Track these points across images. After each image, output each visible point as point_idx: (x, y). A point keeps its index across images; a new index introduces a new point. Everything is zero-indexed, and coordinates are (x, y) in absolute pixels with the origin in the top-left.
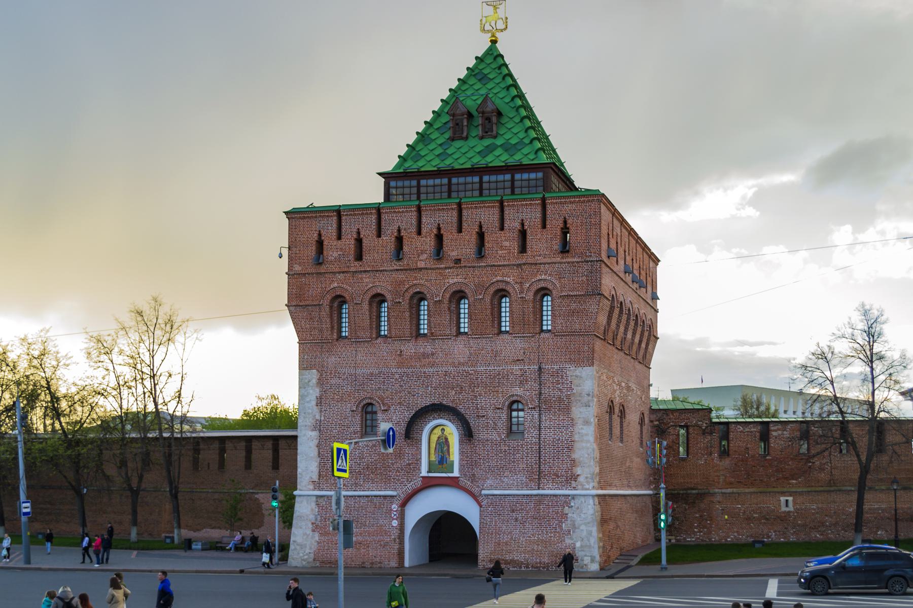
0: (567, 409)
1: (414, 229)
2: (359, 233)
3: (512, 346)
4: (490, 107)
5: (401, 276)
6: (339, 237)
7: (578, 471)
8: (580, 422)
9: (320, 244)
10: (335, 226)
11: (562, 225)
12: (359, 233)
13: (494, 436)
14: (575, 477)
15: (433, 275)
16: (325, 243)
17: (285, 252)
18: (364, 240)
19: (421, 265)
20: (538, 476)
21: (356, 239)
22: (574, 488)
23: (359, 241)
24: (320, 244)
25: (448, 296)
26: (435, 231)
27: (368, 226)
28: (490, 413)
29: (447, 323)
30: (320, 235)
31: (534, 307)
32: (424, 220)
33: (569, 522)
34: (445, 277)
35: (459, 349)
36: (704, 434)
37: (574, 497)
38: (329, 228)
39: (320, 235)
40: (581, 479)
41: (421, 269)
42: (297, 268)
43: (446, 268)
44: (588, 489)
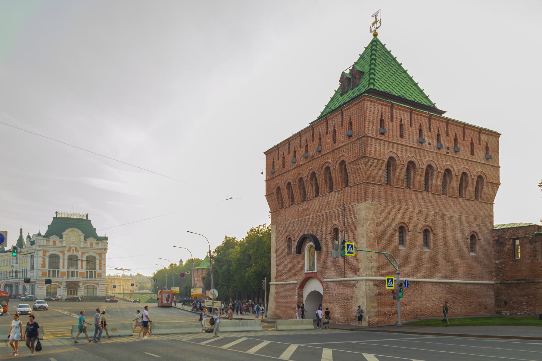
0: (354, 230)
3: (334, 197)
5: (295, 171)
6: (278, 159)
7: (360, 265)
8: (360, 236)
13: (328, 249)
14: (358, 269)
15: (305, 167)
19: (301, 163)
20: (344, 270)
22: (358, 276)
25: (309, 176)
28: (327, 237)
29: (311, 191)
31: (340, 173)
33: (355, 296)
34: (308, 166)
35: (316, 203)
37: (357, 281)
40: (361, 270)
41: (301, 165)
43: (309, 162)
44: (363, 276)
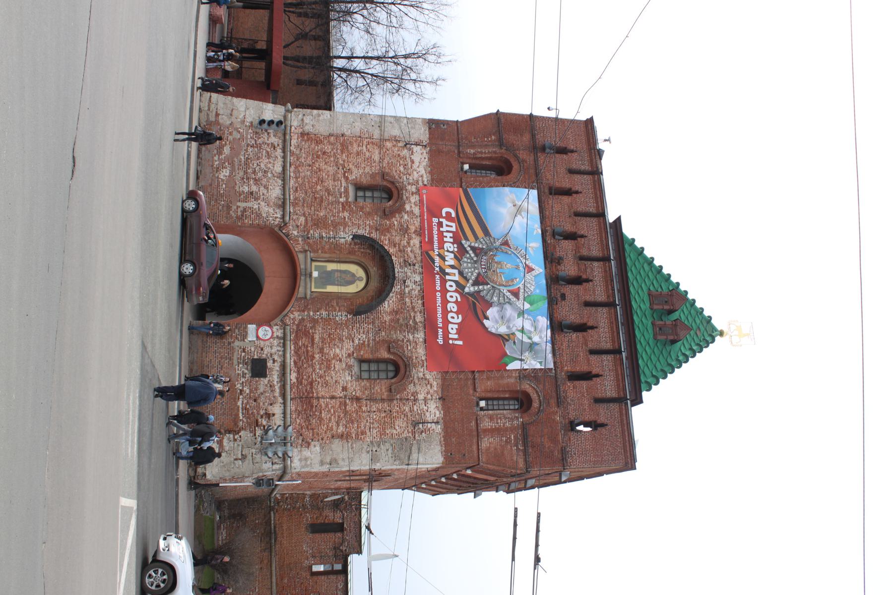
1: (585, 252)
2: (577, 192)
4: (682, 333)
9: (563, 151)
10: (583, 168)
11: (599, 422)
12: (577, 192)
16: (565, 156)
17: (552, 114)
18: (570, 198)
21: (570, 189)
23: (568, 192)
24: (563, 151)
26: (584, 277)
27: (585, 204)
30: (572, 151)
32: (596, 264)
36: (335, 548)
38: (579, 162)
39: (572, 151)
42: (538, 124)
